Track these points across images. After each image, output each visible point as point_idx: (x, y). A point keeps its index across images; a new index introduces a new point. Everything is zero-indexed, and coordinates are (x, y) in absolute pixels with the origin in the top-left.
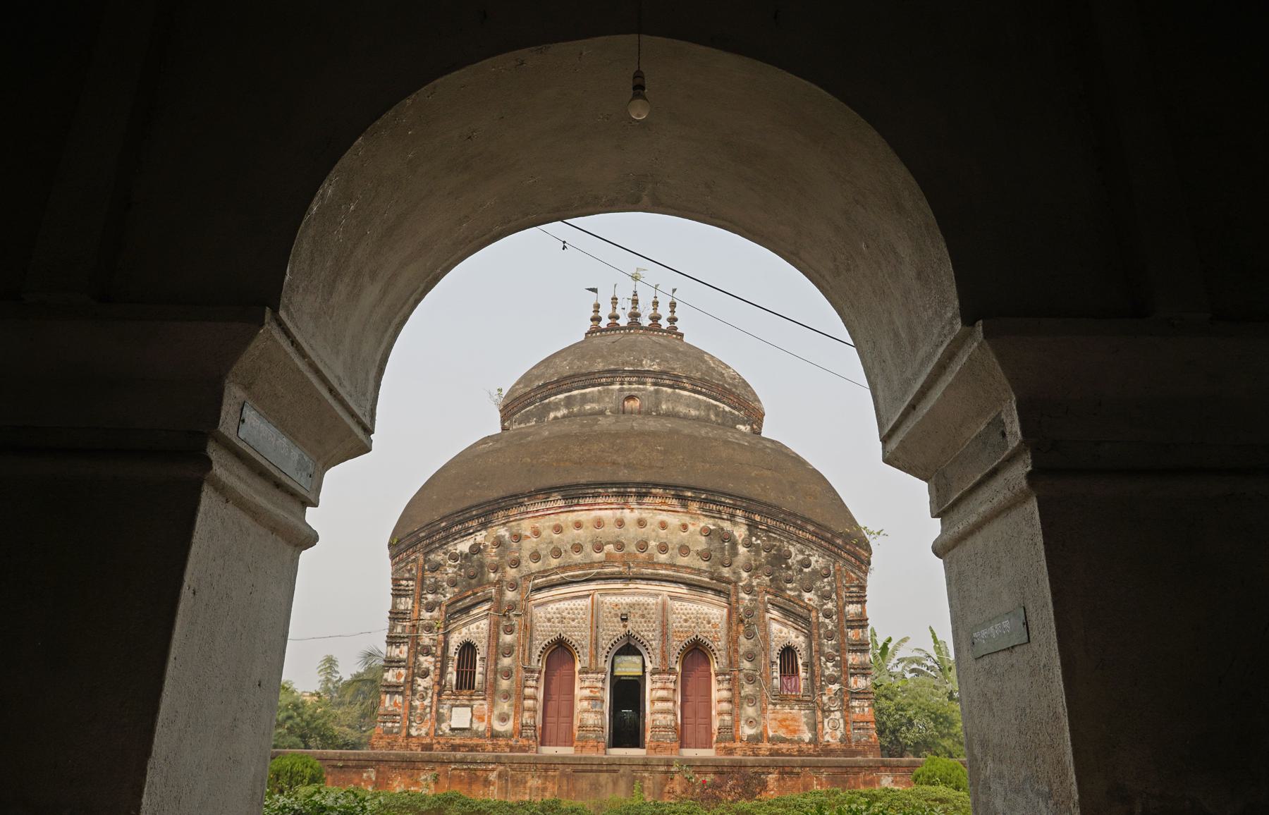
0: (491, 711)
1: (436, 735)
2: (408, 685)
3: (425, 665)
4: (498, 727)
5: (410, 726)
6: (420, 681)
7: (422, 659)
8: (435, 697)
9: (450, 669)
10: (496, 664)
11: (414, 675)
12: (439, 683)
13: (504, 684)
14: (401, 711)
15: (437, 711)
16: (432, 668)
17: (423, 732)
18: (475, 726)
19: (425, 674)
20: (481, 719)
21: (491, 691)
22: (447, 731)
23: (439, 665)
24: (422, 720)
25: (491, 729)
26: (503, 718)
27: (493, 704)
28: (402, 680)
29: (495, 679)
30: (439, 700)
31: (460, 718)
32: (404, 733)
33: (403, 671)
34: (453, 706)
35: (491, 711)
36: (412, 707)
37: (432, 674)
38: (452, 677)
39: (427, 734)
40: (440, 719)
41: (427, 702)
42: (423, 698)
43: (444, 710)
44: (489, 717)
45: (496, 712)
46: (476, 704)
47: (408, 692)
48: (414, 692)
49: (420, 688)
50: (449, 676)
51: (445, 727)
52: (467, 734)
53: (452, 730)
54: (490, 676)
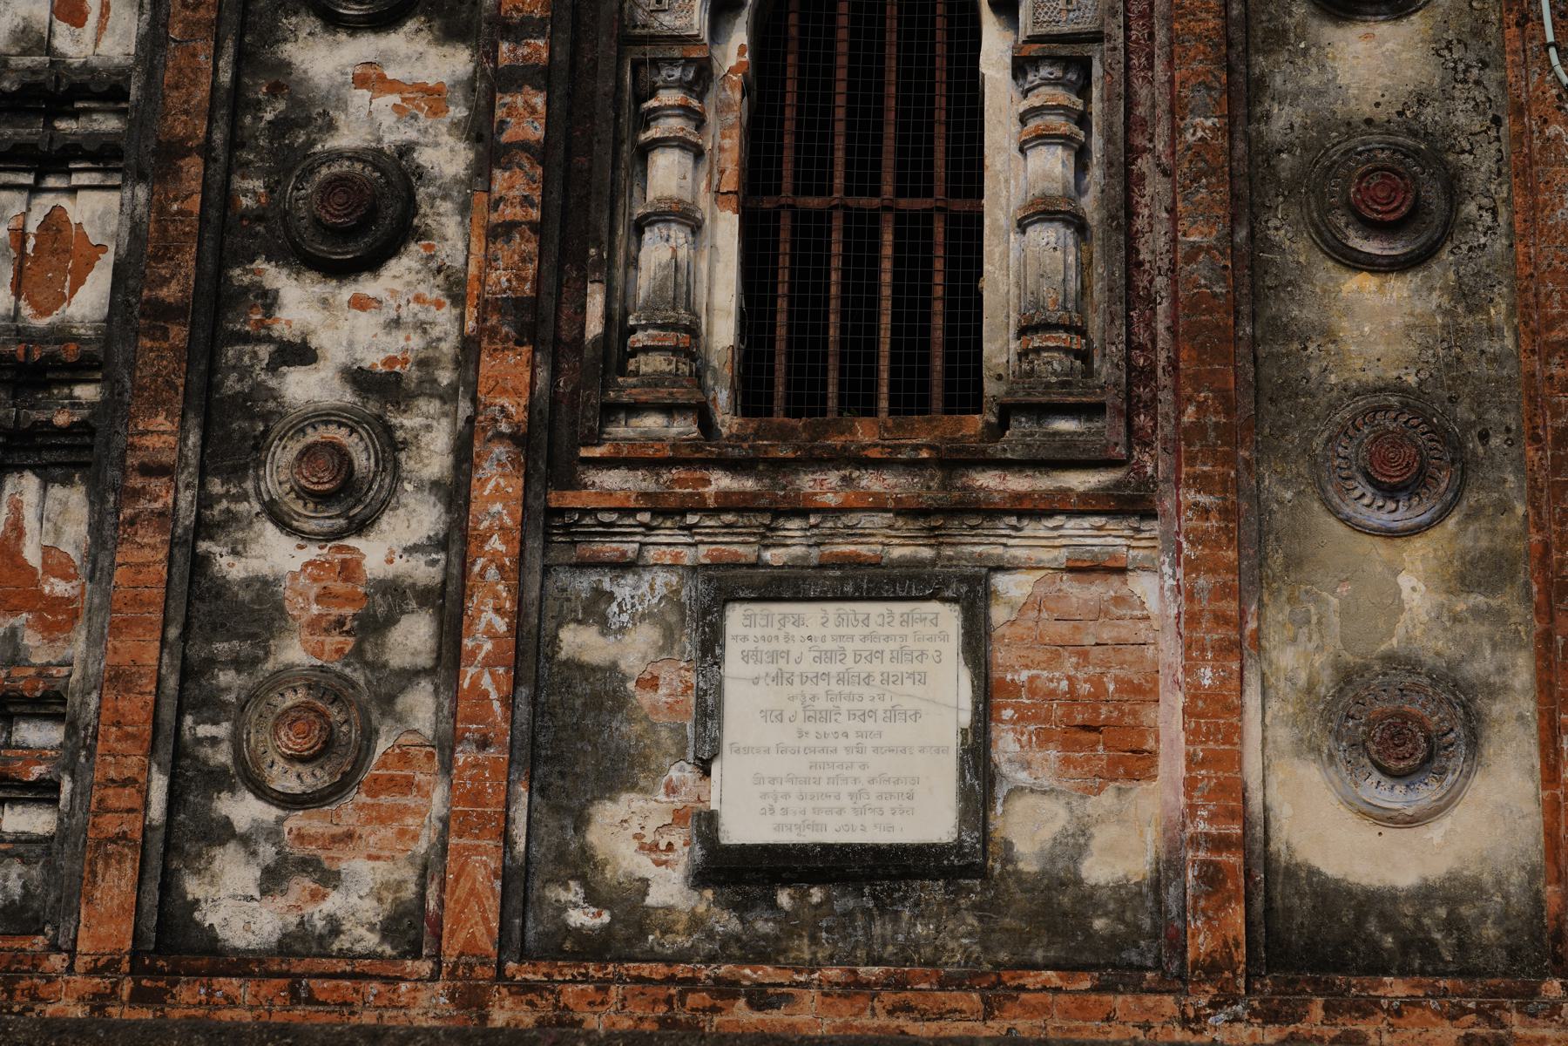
0: (1226, 637)
1: (525, 933)
2: (161, 355)
3: (366, 122)
4: (1332, 830)
5: (187, 836)
6: (299, 302)
7: (321, 58)
8: (498, 489)
9: (667, 174)
10: (1244, 96)
11: (227, 237)
12: (538, 320)
13: (1371, 320)
14: (69, 654)
15: (530, 650)
16: (446, 158)
17: (356, 903)
18: (1029, 829)
19: (365, 221)
20: (1105, 740)
21: (1197, 410)
22: (669, 888)
23: (526, 117)
24: (340, 760)
25: (1240, 857)
26: (1402, 730)
27: (1245, 569)
28: (89, 301)
29: (1252, 271)
30: (552, 528)
31: (831, 723)
32: (108, 913)
33: (95, 210)
34: (727, 586)
35: (1226, 637)
36: (212, 616)
37: (451, 234)
38: (694, 258)
39: (409, 928)
40: (566, 740)
41: (395, 545)
42: (348, 500)
43: (623, 641)
44: (1215, 718)
45: (1295, 657)
46: (1028, 566)
47: (160, 433)
48: (232, 432)
49: (302, 387)
50: (657, 251)
51: (633, 838)
52: (944, 929)
53: (735, 871)
54: (1182, 230)
